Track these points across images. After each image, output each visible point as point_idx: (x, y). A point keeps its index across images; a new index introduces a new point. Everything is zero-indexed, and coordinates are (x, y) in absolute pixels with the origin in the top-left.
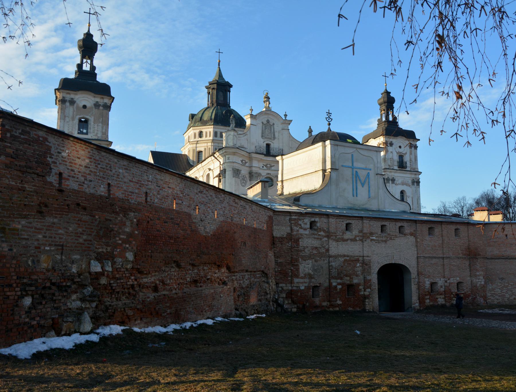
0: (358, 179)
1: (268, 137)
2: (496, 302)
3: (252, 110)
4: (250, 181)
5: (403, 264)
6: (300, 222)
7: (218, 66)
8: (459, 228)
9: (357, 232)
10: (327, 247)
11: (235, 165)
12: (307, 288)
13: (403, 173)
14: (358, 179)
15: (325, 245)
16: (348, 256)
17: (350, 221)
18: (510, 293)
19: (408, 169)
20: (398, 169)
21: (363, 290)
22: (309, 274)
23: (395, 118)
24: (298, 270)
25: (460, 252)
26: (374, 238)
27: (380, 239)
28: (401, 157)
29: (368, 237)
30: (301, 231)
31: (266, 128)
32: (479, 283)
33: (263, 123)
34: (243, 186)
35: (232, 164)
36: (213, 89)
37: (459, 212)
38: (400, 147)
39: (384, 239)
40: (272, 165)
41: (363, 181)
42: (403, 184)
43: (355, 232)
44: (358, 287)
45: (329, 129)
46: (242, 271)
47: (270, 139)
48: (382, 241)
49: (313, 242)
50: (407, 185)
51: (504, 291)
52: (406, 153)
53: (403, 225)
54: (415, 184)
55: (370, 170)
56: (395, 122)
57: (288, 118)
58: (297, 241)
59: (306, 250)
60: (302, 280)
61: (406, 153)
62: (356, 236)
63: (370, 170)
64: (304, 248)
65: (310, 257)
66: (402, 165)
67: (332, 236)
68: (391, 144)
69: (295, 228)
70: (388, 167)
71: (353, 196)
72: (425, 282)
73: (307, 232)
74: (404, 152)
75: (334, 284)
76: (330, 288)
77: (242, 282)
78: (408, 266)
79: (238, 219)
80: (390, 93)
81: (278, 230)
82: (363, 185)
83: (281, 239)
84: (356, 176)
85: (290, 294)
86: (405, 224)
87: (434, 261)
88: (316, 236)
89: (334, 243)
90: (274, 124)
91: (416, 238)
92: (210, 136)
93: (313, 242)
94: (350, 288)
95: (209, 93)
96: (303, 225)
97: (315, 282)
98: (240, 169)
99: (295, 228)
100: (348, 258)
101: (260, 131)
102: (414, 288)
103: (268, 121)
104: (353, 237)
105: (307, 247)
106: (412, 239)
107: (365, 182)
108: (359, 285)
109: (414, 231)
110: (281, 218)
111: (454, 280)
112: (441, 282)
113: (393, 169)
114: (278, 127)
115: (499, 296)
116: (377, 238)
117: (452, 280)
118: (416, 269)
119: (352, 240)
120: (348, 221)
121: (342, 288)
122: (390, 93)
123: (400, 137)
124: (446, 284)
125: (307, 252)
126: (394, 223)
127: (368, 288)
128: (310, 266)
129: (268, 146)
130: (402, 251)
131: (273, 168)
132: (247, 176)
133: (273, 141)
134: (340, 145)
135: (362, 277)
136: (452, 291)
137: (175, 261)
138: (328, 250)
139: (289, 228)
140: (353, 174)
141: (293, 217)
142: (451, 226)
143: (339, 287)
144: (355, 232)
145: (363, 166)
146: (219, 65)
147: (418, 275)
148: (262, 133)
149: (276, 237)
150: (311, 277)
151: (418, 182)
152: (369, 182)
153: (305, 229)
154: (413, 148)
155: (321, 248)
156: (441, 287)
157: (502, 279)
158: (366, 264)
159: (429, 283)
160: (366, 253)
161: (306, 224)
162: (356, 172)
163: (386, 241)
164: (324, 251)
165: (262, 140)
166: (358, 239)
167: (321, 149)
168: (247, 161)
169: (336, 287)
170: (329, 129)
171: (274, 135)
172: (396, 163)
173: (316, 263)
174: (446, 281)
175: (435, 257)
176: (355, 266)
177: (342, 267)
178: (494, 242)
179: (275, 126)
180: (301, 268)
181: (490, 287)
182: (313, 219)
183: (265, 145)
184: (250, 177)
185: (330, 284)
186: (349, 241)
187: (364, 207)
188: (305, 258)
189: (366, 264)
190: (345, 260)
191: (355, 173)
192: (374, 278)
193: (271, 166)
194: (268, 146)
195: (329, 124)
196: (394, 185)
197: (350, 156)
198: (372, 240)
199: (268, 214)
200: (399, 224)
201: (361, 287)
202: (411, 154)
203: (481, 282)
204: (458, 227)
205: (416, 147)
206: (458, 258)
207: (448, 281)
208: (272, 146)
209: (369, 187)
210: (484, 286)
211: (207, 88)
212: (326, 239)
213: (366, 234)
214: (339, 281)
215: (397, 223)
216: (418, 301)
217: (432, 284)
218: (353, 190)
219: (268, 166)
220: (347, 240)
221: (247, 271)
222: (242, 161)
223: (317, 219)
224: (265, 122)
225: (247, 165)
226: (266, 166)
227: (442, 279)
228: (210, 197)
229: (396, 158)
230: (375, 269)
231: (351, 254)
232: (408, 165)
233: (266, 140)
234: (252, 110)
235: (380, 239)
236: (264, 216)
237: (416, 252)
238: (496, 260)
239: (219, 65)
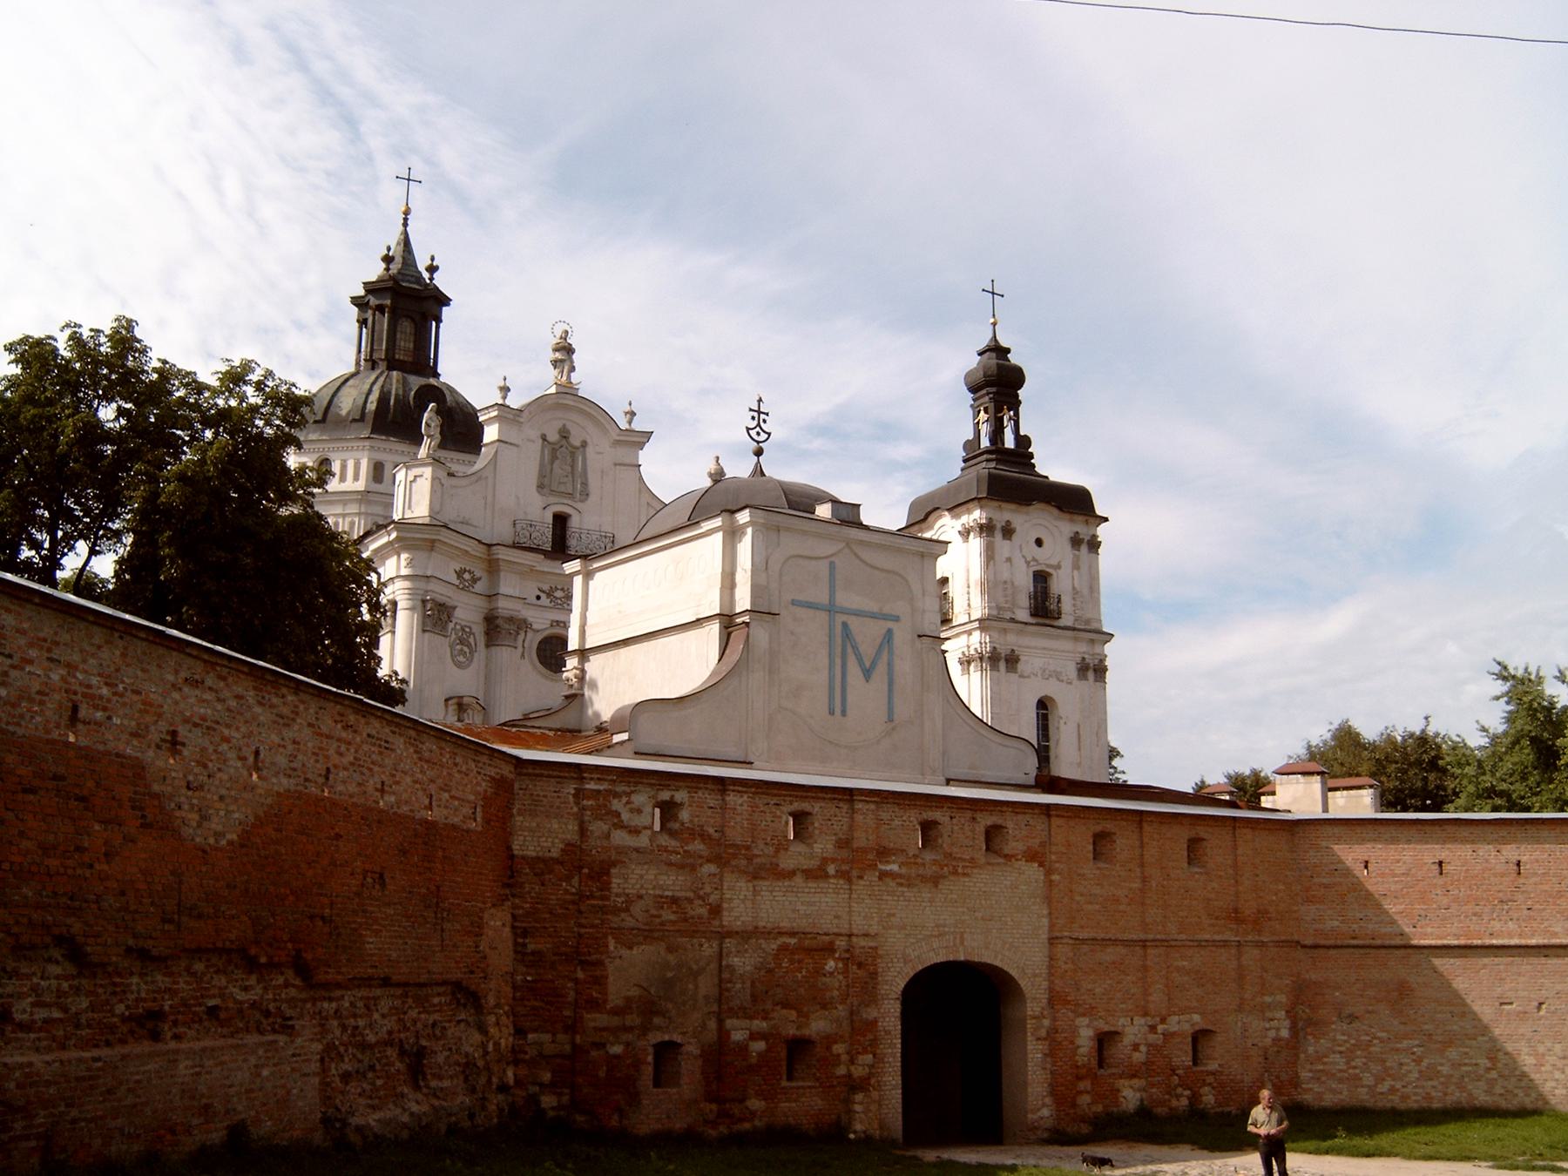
0: (849, 650)
1: (562, 489)
2: (1329, 1100)
3: (505, 390)
4: (488, 646)
5: (997, 963)
6: (616, 805)
7: (401, 228)
8: (1202, 835)
9: (830, 846)
10: (713, 898)
11: (433, 586)
13: (1050, 637)
14: (849, 650)
15: (708, 889)
16: (792, 934)
17: (805, 806)
18: (1376, 1068)
19: (1063, 622)
20: (1031, 620)
21: (844, 1057)
23: (1023, 442)
24: (600, 981)
26: (894, 867)
27: (913, 872)
28: (1041, 578)
29: (873, 867)
30: (620, 838)
31: (554, 458)
32: (1272, 1034)
34: (459, 665)
35: (422, 585)
36: (380, 309)
38: (1039, 542)
39: (930, 870)
41: (868, 665)
42: (1048, 675)
44: (829, 1048)
45: (759, 471)
46: (366, 982)
47: (571, 495)
48: (923, 879)
49: (663, 880)
50: (1058, 676)
51: (1358, 1062)
52: (1058, 567)
53: (1000, 822)
54: (1091, 675)
55: (897, 619)
56: (1022, 454)
57: (638, 425)
58: (601, 873)
59: (637, 909)
61: (1058, 567)
62: (825, 861)
63: (897, 619)
64: (629, 901)
65: (649, 934)
66: (1043, 607)
67: (735, 856)
68: (1008, 532)
69: (598, 827)
70: (995, 612)
71: (832, 713)
72: (1074, 1031)
73: (643, 841)
74: (1054, 562)
75: (738, 1036)
77: (361, 1023)
78: (1014, 973)
79: (352, 788)
80: (1008, 351)
81: (530, 830)
82: (867, 674)
83: (542, 866)
87: (1110, 954)
88: (673, 858)
89: (742, 884)
90: (584, 444)
91: (1048, 873)
92: (356, 478)
93: (663, 880)
94: (799, 1047)
95: (362, 322)
96: (625, 816)
98: (450, 603)
99: (598, 827)
100: (793, 941)
102: (1035, 1052)
103: (564, 434)
104: (814, 863)
105: (640, 897)
106: (1033, 872)
107: (874, 663)
108: (830, 1040)
109: (1042, 844)
110: (544, 789)
111: (1181, 1024)
112: (1133, 1031)
113: (1013, 620)
114: (598, 457)
115: (1341, 1081)
116: (904, 871)
117: (1173, 1024)
118: (1045, 984)
119: (809, 874)
120: (797, 806)
121: (769, 1050)
122: (1008, 351)
123: (1037, 506)
124: (1152, 1038)
126: (969, 814)
127: (865, 1052)
129: (561, 521)
132: (479, 630)
133: (579, 506)
134: (788, 529)
135: (841, 1011)
136: (1176, 1061)
137: (60, 940)
138: (716, 911)
139: (573, 826)
140: (831, 636)
141: (591, 786)
143: (759, 1046)
144: (823, 846)
145: (873, 607)
146: (405, 224)
147: (1051, 1002)
148: (542, 476)
149: (523, 857)
151: (1100, 671)
152: (890, 665)
153: (635, 831)
154: (1084, 548)
155: (690, 901)
156: (1136, 1047)
157: (1352, 1018)
158: (860, 965)
159: (1091, 1033)
160: (859, 924)
161: (639, 811)
162: (845, 625)
164: (703, 911)
166: (831, 869)
167: (718, 537)
168: (478, 574)
170: (759, 471)
171: (585, 484)
172: (1024, 601)
173: (671, 958)
174: (1153, 1029)
176: (819, 972)
177: (770, 971)
178: (1326, 886)
179: (590, 450)
182: (665, 795)
183: (550, 520)
184: (487, 633)
185: (723, 1034)
186: (799, 880)
188: (629, 939)
189: (863, 967)
190: (784, 948)
191: (839, 629)
192: (889, 1016)
194: (561, 521)
195: (759, 453)
196: (1013, 677)
197: (823, 567)
198: (883, 875)
199: (492, 772)
200: (986, 820)
201: (839, 1048)
202: (1076, 566)
203: (1278, 1029)
205: (1094, 545)
206: (1200, 944)
207: (1160, 1028)
208: (574, 523)
211: (356, 301)
212: (711, 868)
213: (865, 851)
214: (760, 1025)
215: (978, 816)
216: (1048, 1100)
217: (1105, 1040)
219: (559, 594)
220: (791, 874)
221: (386, 982)
222: (459, 574)
223: (681, 796)
224: (553, 437)
225: (479, 587)
226: (549, 595)
227: (1139, 1021)
228: (233, 703)
229: (1025, 582)
230: (895, 980)
231: (802, 924)
232: (1066, 606)
233: (552, 499)
234: (505, 390)
235: (913, 872)
236: (472, 783)
237: (1045, 921)
238: (1332, 952)
239: (405, 224)
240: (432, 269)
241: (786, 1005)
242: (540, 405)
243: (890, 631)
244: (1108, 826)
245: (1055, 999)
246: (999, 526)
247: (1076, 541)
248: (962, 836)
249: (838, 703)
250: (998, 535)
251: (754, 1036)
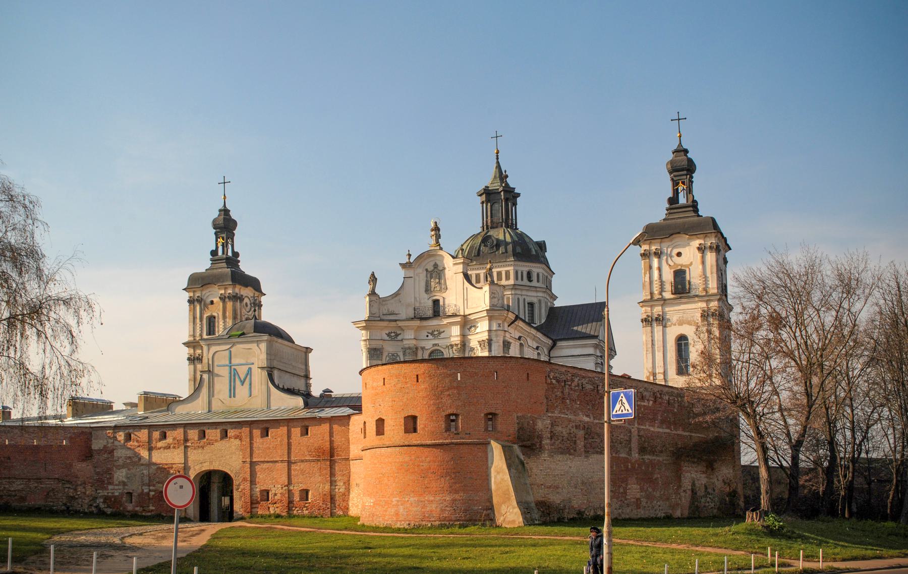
3: (410, 255)
12: (122, 494)
13: (685, 303)
19: (693, 293)
20: (672, 296)
22: (123, 482)
25: (307, 453)
28: (680, 274)
30: (116, 443)
33: (427, 270)
37: (654, 375)
39: (202, 444)
40: (442, 330)
42: (681, 323)
43: (169, 440)
47: (440, 291)
52: (691, 264)
58: (112, 452)
60: (116, 487)
61: (691, 264)
65: (123, 467)
68: (658, 254)
75: (146, 491)
76: (142, 494)
82: (243, 383)
83: (99, 451)
84: (233, 374)
85: (106, 499)
86: (228, 427)
87: (265, 466)
90: (444, 268)
97: (129, 488)
98: (378, 347)
101: (423, 284)
106: (237, 442)
107: (245, 380)
117: (291, 488)
119: (165, 448)
125: (121, 462)
128: (124, 474)
129: (436, 302)
130: (226, 456)
131: (442, 335)
133: (444, 295)
138: (140, 459)
140: (230, 373)
142: (295, 424)
143: (152, 493)
150: (124, 484)
163: (203, 447)
165: (426, 296)
168: (398, 332)
169: (148, 494)
172: (668, 287)
175: (268, 462)
179: (446, 271)
180: (116, 476)
181: (353, 495)
187: (242, 408)
193: (440, 333)
200: (222, 427)
202: (703, 263)
204: (307, 423)
206: (302, 461)
209: (251, 384)
210: (344, 494)
214: (151, 488)
218: (230, 390)
220: (160, 449)
222: (388, 335)
224: (430, 268)
225: (399, 338)
229: (668, 276)
234: (410, 255)
239: (498, 162)
240: (507, 176)
241: (159, 483)
242: (421, 257)
243: (250, 369)
244: (267, 425)
245: (244, 479)
246: (652, 252)
247: (701, 249)
248: (213, 434)
249: (232, 393)
251: (150, 491)
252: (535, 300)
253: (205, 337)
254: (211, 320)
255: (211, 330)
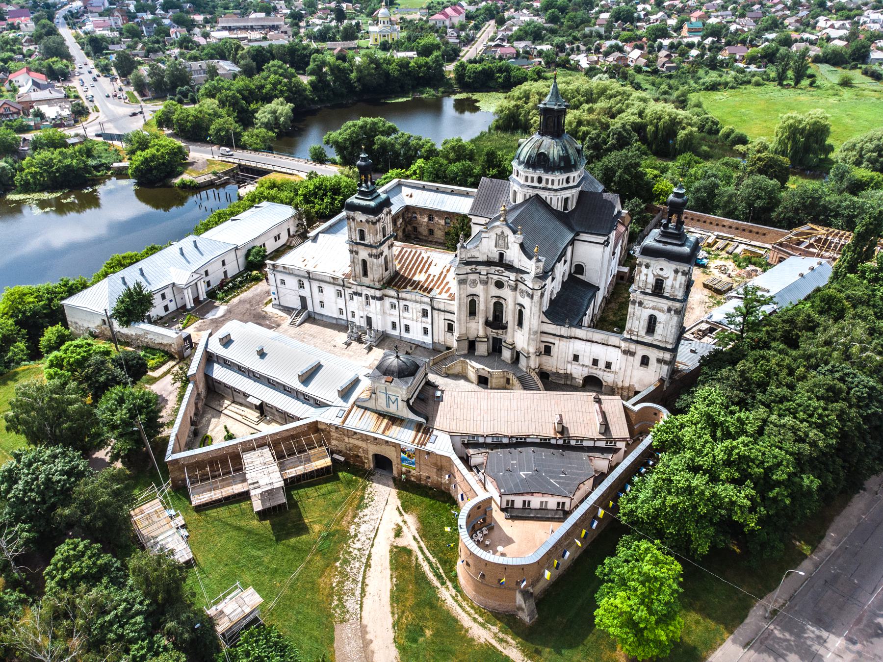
42: (654, 308)
54: (673, 312)
68: (647, 266)
103: (503, 233)
129: (501, 255)
154: (680, 274)
165: (496, 249)
194: (501, 255)
202: (675, 279)
224: (499, 233)
229: (651, 280)
247: (676, 272)
249: (388, 405)
250: (643, 267)
252: (569, 195)
253: (358, 241)
254: (362, 232)
255: (362, 237)
